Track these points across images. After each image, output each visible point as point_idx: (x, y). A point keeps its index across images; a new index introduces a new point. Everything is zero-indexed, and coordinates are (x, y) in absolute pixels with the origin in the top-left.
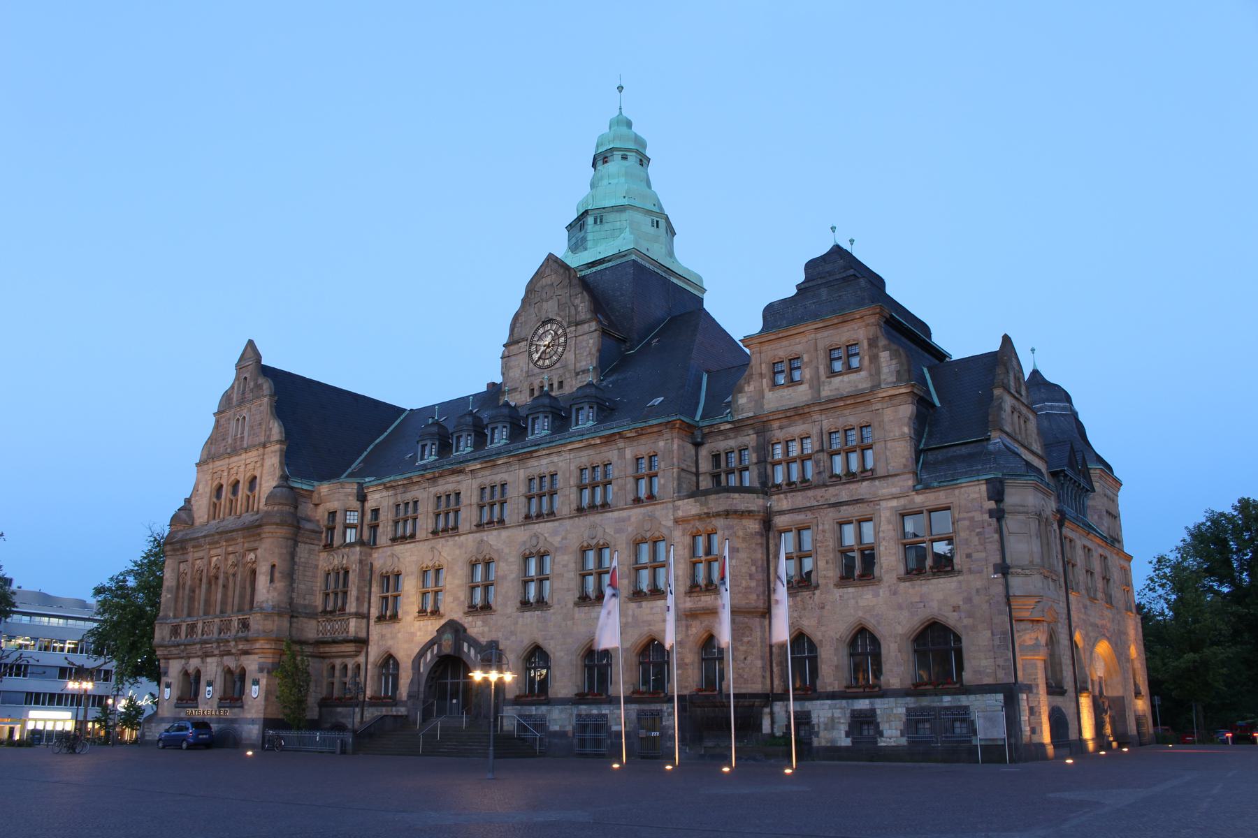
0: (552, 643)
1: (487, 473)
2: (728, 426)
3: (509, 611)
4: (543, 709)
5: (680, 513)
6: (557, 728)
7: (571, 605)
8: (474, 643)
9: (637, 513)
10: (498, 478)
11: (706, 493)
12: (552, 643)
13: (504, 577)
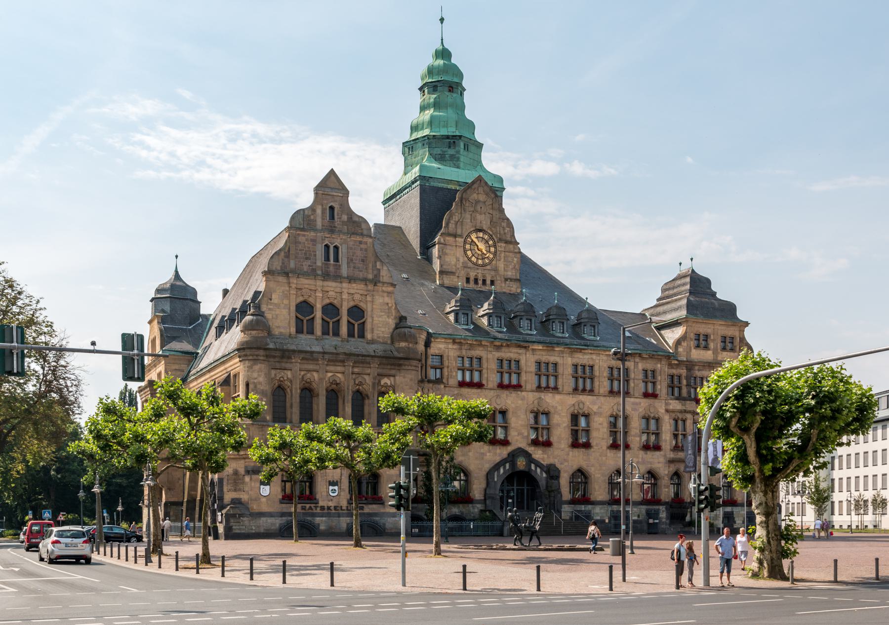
0: (593, 469)
1: (544, 353)
2: (676, 362)
3: (563, 446)
4: (589, 507)
5: (671, 407)
6: (598, 518)
7: (605, 448)
8: (538, 464)
9: (645, 402)
10: (552, 359)
11: (685, 399)
12: (593, 469)
13: (558, 425)
